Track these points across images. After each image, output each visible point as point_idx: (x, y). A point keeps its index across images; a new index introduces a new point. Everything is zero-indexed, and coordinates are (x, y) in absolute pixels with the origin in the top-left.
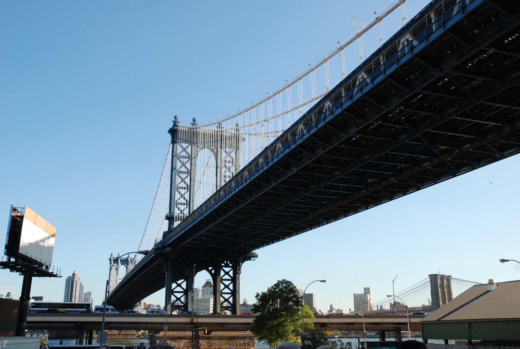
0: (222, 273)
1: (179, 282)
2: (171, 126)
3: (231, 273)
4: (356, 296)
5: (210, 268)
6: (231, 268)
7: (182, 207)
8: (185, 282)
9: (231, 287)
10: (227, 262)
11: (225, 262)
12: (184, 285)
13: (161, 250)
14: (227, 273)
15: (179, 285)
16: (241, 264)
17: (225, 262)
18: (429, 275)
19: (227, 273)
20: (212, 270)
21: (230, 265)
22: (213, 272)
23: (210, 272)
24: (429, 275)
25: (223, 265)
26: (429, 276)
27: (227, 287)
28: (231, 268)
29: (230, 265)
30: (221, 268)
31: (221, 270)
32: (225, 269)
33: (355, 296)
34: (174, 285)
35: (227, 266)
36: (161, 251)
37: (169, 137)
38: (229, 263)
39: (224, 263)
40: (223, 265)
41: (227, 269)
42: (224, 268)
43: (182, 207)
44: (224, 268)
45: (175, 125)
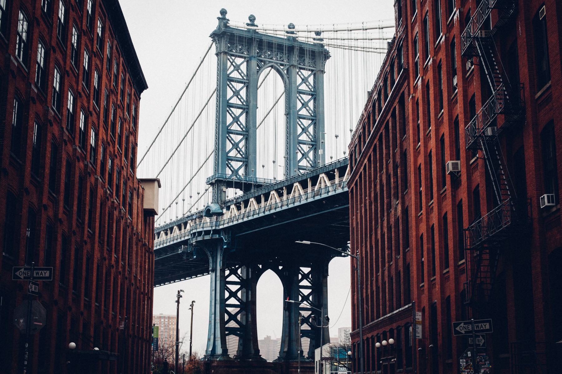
2: (214, 25)
41: (306, 270)
43: (236, 165)
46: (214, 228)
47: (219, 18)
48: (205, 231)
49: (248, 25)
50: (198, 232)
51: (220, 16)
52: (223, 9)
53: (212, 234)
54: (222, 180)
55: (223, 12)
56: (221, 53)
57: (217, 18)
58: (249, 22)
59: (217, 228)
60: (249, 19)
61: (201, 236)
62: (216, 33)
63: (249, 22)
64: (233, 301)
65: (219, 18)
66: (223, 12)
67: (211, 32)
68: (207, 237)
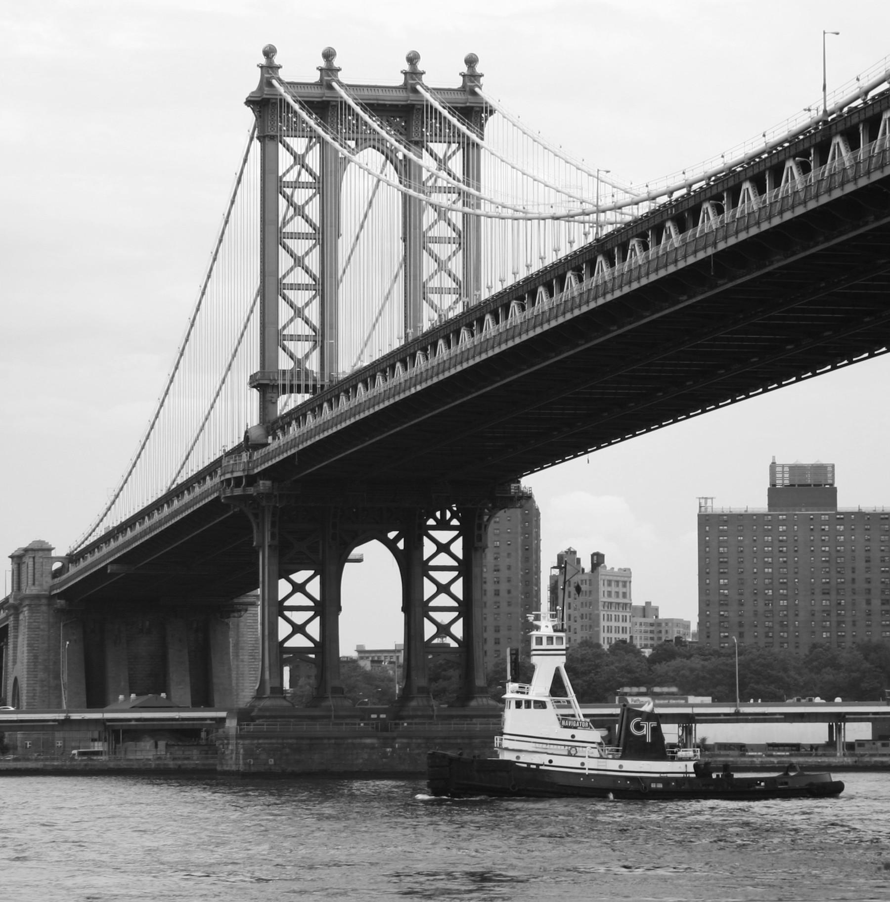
0: (429, 548)
1: (300, 577)
2: (252, 83)
3: (457, 548)
5: (392, 535)
6: (456, 533)
7: (300, 349)
8: (318, 577)
9: (458, 589)
10: (443, 515)
11: (438, 514)
12: (314, 588)
13: (241, 489)
14: (443, 548)
15: (299, 588)
16: (486, 518)
17: (438, 514)
19: (443, 548)
20: (397, 539)
21: (455, 522)
22: (401, 545)
23: (391, 545)
25: (431, 522)
27: (443, 589)
28: (456, 533)
29: (455, 522)
30: (424, 531)
31: (425, 539)
32: (437, 534)
34: (284, 587)
35: (443, 525)
36: (244, 490)
37: (249, 117)
38: (448, 515)
39: (435, 519)
40: (431, 522)
41: (443, 536)
42: (432, 533)
45: (266, 83)
46: (246, 473)
48: (235, 478)
53: (244, 487)
54: (268, 385)
55: (269, 53)
59: (252, 473)
62: (252, 99)
64: (299, 599)
66: (269, 53)
67: (246, 95)
68: (238, 492)
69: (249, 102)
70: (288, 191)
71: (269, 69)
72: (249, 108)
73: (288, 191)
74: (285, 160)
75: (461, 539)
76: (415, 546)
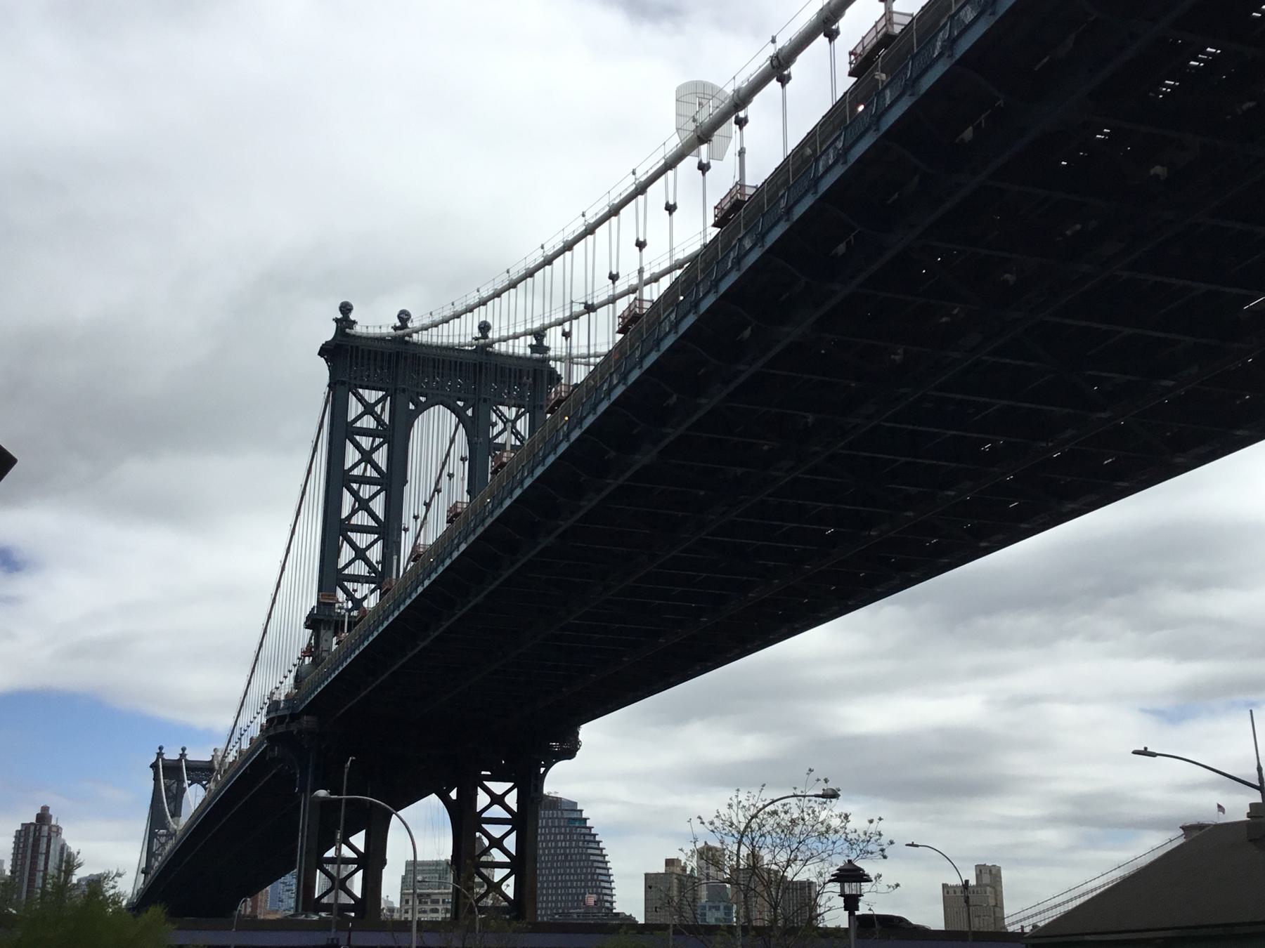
0: (482, 799)
2: (329, 333)
3: (512, 800)
4: (951, 892)
9: (510, 843)
14: (497, 800)
16: (542, 770)
18: (1182, 828)
19: (497, 800)
24: (1182, 828)
26: (1182, 832)
31: (480, 790)
33: (948, 892)
41: (498, 787)
42: (488, 784)
43: (362, 590)
44: (488, 784)
47: (337, 320)
49: (395, 328)
50: (279, 717)
51: (340, 316)
52: (342, 303)
55: (346, 308)
56: (335, 384)
57: (334, 320)
58: (398, 324)
60: (399, 317)
61: (283, 723)
63: (398, 324)
65: (337, 320)
66: (346, 308)
69: (321, 353)
70: (355, 486)
71: (344, 322)
72: (323, 359)
73: (355, 486)
74: (355, 408)
75: (515, 791)
76: (468, 798)
